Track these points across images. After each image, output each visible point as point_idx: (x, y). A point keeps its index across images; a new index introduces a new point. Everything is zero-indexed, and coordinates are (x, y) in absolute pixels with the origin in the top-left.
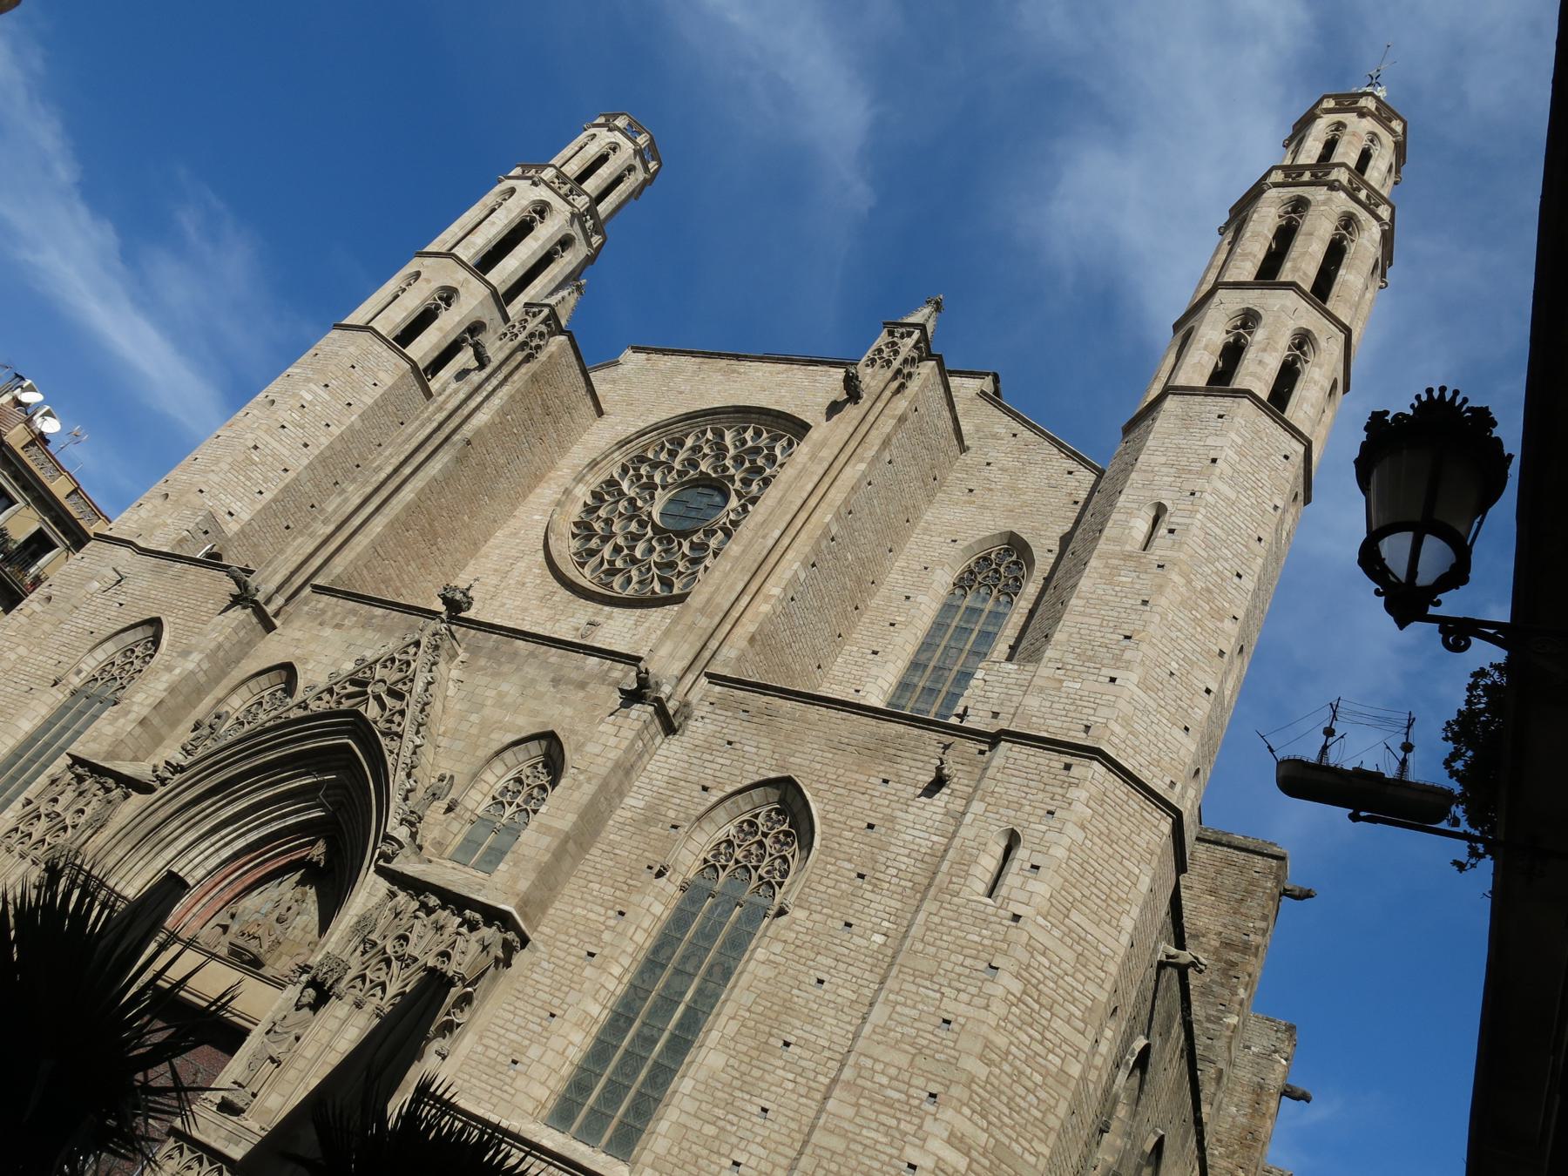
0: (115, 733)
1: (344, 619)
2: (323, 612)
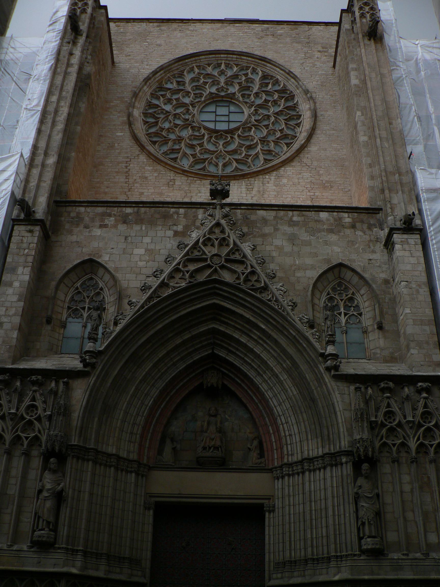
0: (3, 342)
1: (103, 220)
2: (82, 219)
